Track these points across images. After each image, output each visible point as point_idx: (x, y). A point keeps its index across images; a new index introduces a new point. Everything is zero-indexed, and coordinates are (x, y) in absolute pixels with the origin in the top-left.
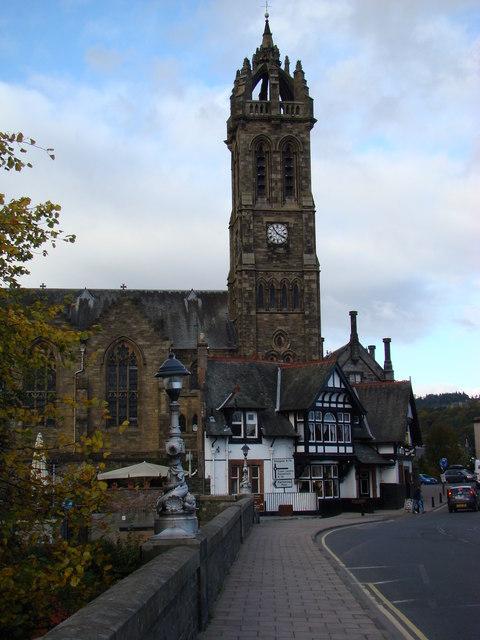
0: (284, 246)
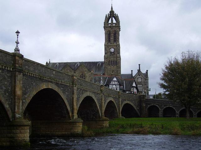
0: (114, 52)
